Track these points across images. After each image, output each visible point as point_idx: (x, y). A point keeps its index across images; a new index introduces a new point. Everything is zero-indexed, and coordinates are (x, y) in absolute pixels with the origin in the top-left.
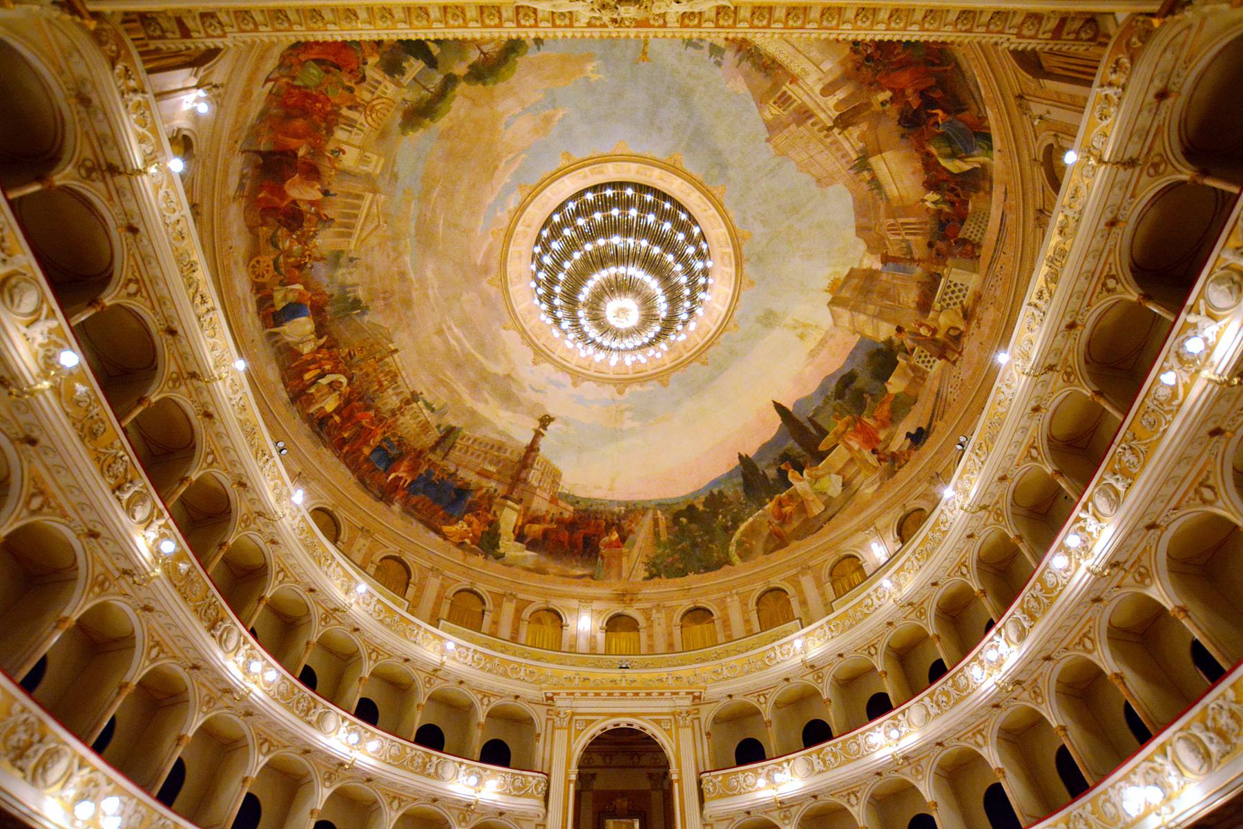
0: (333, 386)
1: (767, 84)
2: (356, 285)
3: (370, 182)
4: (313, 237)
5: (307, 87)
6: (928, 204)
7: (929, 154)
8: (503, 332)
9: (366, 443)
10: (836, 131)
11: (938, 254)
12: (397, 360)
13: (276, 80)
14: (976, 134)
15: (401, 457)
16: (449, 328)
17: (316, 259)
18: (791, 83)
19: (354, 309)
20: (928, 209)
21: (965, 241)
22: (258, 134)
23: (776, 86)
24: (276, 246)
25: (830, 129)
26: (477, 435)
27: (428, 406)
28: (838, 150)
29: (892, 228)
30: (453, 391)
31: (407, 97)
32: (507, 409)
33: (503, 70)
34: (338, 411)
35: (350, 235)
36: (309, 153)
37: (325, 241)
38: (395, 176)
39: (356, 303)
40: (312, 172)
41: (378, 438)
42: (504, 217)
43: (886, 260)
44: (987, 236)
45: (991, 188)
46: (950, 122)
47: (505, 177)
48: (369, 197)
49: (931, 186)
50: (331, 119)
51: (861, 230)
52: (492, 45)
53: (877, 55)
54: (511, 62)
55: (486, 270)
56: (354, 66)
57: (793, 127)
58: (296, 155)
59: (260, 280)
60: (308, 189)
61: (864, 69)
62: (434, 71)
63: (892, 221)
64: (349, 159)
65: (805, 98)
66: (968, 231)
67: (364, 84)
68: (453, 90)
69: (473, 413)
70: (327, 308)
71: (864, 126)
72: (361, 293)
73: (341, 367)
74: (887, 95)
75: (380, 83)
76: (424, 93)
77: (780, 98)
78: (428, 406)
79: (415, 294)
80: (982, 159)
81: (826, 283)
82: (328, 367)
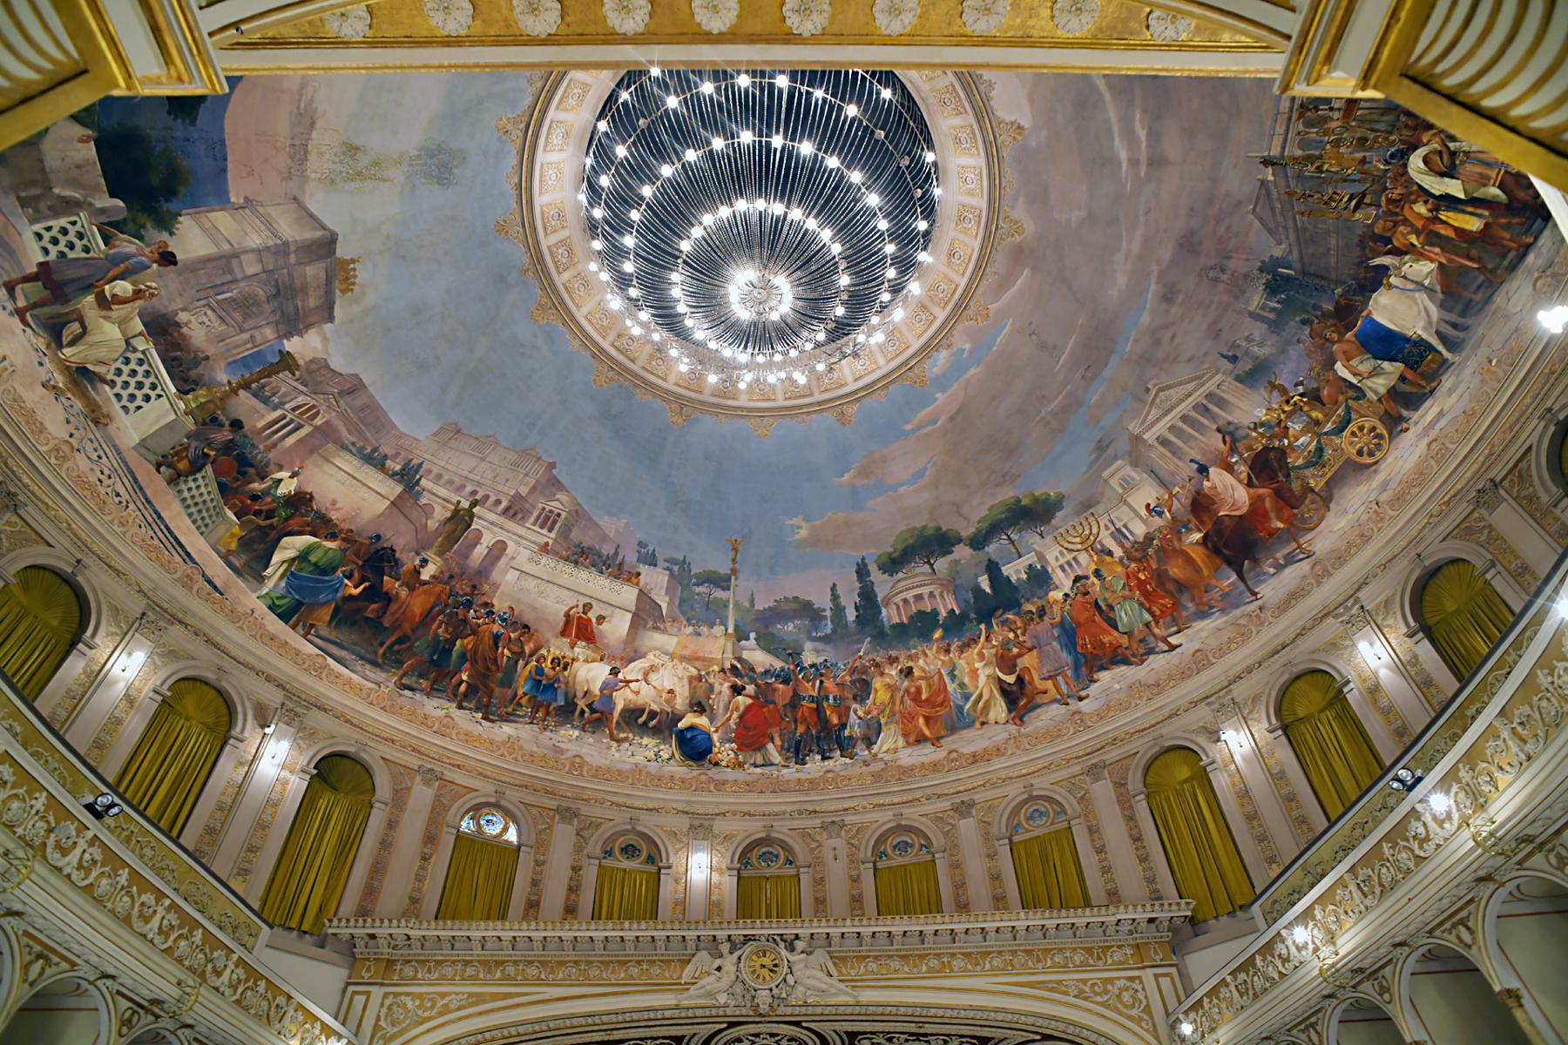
1: (576, 535)
2: (1254, 316)
4: (1262, 425)
5: (1141, 605)
6: (284, 474)
7: (332, 536)
8: (1026, 123)
10: (465, 504)
11: (214, 420)
12: (1277, 142)
13: (1165, 641)
14: (300, 604)
16: (1134, 162)
17: (1283, 391)
18: (547, 544)
19: (1287, 278)
20: (281, 468)
21: (196, 468)
22: (1225, 596)
23: (565, 533)
24: (1320, 450)
25: (474, 504)
28: (451, 482)
29: (312, 412)
33: (911, 541)
35: (1209, 396)
36: (1189, 530)
38: (1101, 447)
40: (1201, 505)
43: (286, 362)
44: (177, 507)
45: (230, 565)
46: (337, 591)
49: (300, 500)
50: (1138, 551)
51: (354, 387)
53: (461, 611)
54: (900, 547)
55: (1019, 255)
57: (524, 491)
58: (1205, 538)
59: (1381, 430)
61: (468, 590)
62: (993, 557)
63: (318, 421)
64: (1149, 493)
65: (521, 531)
66: (204, 485)
67: (1080, 573)
71: (433, 524)
72: (1256, 298)
74: (426, 575)
75: (1062, 567)
77: (555, 522)
79: (1166, 252)
80: (270, 584)
81: (362, 275)
82: (1421, 208)
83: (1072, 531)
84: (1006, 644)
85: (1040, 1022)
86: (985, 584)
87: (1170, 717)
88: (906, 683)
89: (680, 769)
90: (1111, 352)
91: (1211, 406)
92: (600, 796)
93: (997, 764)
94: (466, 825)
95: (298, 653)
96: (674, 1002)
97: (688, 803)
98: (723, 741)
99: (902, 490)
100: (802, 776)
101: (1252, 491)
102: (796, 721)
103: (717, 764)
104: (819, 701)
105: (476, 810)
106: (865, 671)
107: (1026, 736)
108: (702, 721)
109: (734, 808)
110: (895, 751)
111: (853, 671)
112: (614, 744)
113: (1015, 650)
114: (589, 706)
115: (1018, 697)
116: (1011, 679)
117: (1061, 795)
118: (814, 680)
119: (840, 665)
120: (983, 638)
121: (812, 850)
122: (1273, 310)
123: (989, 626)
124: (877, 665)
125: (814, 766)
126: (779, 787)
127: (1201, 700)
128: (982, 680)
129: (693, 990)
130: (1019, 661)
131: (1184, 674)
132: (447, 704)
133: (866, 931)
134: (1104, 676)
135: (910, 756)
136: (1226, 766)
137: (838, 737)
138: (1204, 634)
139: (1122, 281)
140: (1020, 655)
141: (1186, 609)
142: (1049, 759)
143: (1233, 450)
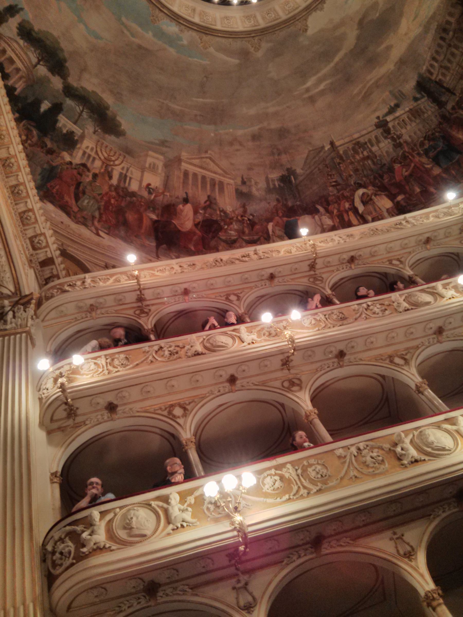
0: (366, 201)
2: (267, 178)
3: (172, 163)
4: (225, 212)
5: (99, 209)
8: (310, 32)
9: (428, 171)
13: (97, 229)
15: (447, 138)
16: (308, 90)
17: (245, 211)
19: (290, 182)
26: (428, 58)
27: (392, 110)
30: (377, 85)
31: (91, 130)
32: (397, 23)
33: (48, 42)
34: (392, 197)
35: (221, 184)
36: (154, 212)
37: (228, 203)
38: (163, 143)
39: (285, 179)
40: (169, 210)
41: (424, 160)
42: (187, 37)
47: (148, 37)
48: (184, 166)
50: (122, 192)
52: (30, 54)
56: (75, 172)
60: (184, 213)
62: (64, 106)
64: (155, 181)
67: (89, 165)
68: (76, 89)
69: (402, 62)
70: (290, 204)
72: (275, 175)
73: (347, 194)
75: (84, 153)
76: (85, 115)
78: (392, 110)
79: (274, 125)
83: (108, 150)
86: (45, 106)
90: (215, 124)
91: (217, 187)
99: (82, 26)
101: (194, 228)
122: (274, 185)
139: (252, 111)
143: (205, 208)
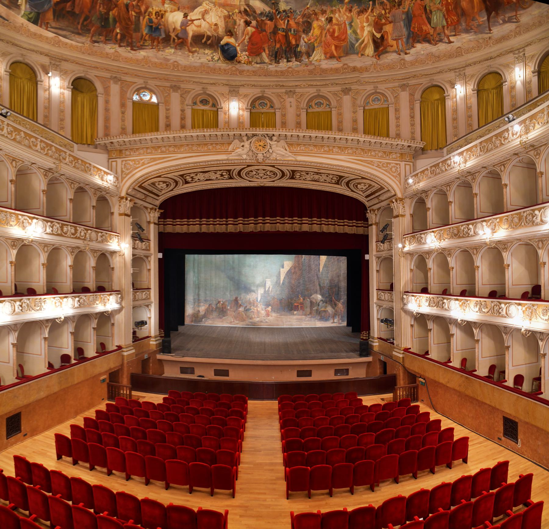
5: (444, 16)
22: (479, 25)
84: (380, 16)
85: (362, 173)
87: (439, 72)
88: (328, 26)
89: (223, 65)
92: (188, 79)
93: (365, 75)
94: (136, 98)
95: (47, 38)
96: (226, 158)
97: (228, 80)
98: (243, 50)
100: (278, 69)
102: (275, 41)
103: (239, 62)
104: (287, 31)
105: (138, 91)
106: (309, 16)
107: (379, 65)
108: (232, 40)
109: (248, 83)
110: (320, 60)
111: (304, 16)
112: (191, 54)
113: (383, 21)
114: (177, 36)
115: (380, 45)
116: (378, 35)
117: (388, 94)
118: (284, 19)
119: (298, 12)
120: (370, 10)
121: (281, 102)
123: (374, 4)
124: (316, 14)
125: (283, 65)
126: (267, 74)
127: (453, 70)
128: (366, 33)
129: (233, 154)
130: (384, 27)
131: (450, 56)
132: (114, 46)
133: (301, 135)
134: (419, 46)
135: (326, 64)
136: (453, 98)
137: (295, 51)
138: (464, 41)
140: (385, 24)
141: (461, 25)
142: (387, 77)
